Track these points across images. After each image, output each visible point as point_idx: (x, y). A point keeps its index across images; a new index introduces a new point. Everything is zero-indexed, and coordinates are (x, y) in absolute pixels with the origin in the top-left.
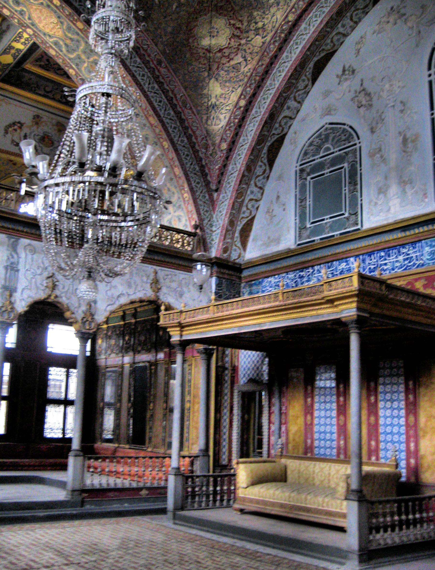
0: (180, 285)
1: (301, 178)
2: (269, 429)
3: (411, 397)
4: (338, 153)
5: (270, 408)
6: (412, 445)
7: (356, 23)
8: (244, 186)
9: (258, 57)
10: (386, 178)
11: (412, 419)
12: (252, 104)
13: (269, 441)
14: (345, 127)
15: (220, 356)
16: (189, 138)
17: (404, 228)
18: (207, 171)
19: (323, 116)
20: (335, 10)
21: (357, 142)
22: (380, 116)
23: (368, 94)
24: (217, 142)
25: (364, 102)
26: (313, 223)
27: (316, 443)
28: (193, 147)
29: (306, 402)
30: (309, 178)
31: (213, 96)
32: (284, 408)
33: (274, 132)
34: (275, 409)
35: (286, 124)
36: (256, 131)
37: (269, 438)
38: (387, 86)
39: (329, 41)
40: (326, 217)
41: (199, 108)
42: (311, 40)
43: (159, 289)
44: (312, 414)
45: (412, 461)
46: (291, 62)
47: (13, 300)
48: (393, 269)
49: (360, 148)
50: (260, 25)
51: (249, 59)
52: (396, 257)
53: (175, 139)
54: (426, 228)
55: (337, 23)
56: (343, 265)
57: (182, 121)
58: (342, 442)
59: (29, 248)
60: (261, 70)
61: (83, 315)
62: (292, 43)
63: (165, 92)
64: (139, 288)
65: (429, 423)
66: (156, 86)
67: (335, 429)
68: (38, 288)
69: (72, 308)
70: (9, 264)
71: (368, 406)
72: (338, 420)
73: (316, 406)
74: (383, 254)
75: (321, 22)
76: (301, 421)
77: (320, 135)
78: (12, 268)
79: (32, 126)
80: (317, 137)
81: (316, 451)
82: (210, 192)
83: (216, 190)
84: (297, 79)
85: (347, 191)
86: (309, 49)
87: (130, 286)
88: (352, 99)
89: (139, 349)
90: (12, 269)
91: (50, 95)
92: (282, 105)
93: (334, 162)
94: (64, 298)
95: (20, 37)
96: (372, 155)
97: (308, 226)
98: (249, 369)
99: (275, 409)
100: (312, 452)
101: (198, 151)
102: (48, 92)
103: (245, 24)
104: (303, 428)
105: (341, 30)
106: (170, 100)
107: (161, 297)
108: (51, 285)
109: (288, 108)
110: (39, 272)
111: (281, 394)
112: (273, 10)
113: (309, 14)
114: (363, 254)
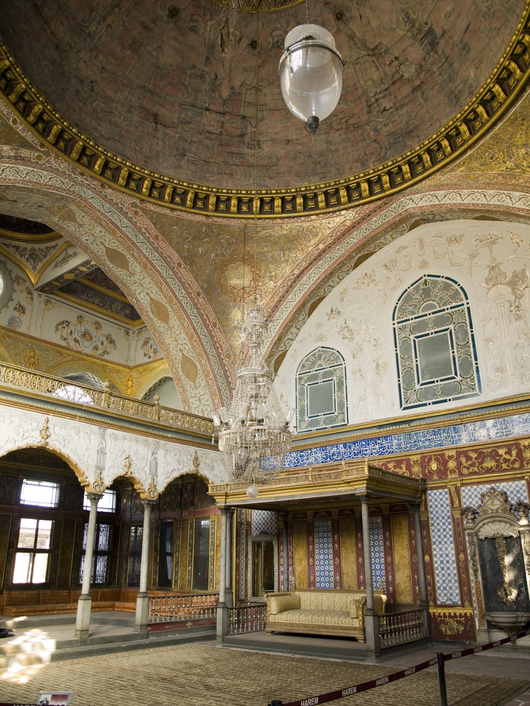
0: (212, 461)
2: (279, 569)
3: (388, 543)
4: (329, 369)
5: (279, 553)
6: (390, 577)
7: (341, 280)
9: (270, 296)
10: (365, 391)
11: (389, 559)
13: (279, 579)
15: (239, 514)
16: (217, 349)
17: (380, 427)
18: (228, 374)
19: (316, 341)
20: (329, 272)
21: (343, 363)
22: (360, 347)
23: (350, 330)
24: (237, 353)
25: (347, 336)
26: (310, 417)
27: (317, 579)
28: (219, 356)
29: (308, 548)
31: (236, 320)
32: (290, 553)
33: (280, 349)
34: (284, 554)
35: (288, 343)
37: (279, 577)
38: (364, 327)
39: (322, 290)
41: (225, 328)
42: (311, 290)
43: (198, 465)
44: (313, 558)
45: (391, 588)
47: (102, 476)
48: (372, 454)
50: (273, 274)
52: (374, 446)
53: (208, 351)
54: (394, 428)
55: (329, 280)
56: (335, 449)
57: (212, 337)
58: (338, 578)
59: (112, 436)
60: (272, 304)
61: (149, 487)
62: (296, 288)
63: (201, 315)
64: (186, 465)
65: (401, 561)
66: (196, 311)
67: (332, 568)
68: (119, 467)
69: (142, 482)
70: (99, 448)
71: (357, 551)
72: (334, 561)
73: (317, 551)
74: (364, 443)
75: (318, 278)
76: (305, 563)
77: (315, 354)
78: (102, 452)
79: (76, 325)
80: (312, 356)
81: (318, 585)
84: (299, 314)
86: (309, 295)
87: (179, 463)
88: (339, 332)
89: (165, 508)
90: (102, 452)
91: (91, 300)
92: (287, 331)
93: (325, 375)
94: (136, 474)
95: (87, 264)
96: (354, 373)
97: (306, 419)
98: (260, 524)
99: (284, 554)
100: (314, 586)
101: (223, 359)
102: (89, 298)
103: (263, 272)
104: (306, 568)
105: (331, 284)
106: (204, 321)
107: (200, 471)
108: (128, 464)
109: (291, 333)
110: (119, 454)
111: (288, 543)
112: (283, 265)
114: (349, 443)
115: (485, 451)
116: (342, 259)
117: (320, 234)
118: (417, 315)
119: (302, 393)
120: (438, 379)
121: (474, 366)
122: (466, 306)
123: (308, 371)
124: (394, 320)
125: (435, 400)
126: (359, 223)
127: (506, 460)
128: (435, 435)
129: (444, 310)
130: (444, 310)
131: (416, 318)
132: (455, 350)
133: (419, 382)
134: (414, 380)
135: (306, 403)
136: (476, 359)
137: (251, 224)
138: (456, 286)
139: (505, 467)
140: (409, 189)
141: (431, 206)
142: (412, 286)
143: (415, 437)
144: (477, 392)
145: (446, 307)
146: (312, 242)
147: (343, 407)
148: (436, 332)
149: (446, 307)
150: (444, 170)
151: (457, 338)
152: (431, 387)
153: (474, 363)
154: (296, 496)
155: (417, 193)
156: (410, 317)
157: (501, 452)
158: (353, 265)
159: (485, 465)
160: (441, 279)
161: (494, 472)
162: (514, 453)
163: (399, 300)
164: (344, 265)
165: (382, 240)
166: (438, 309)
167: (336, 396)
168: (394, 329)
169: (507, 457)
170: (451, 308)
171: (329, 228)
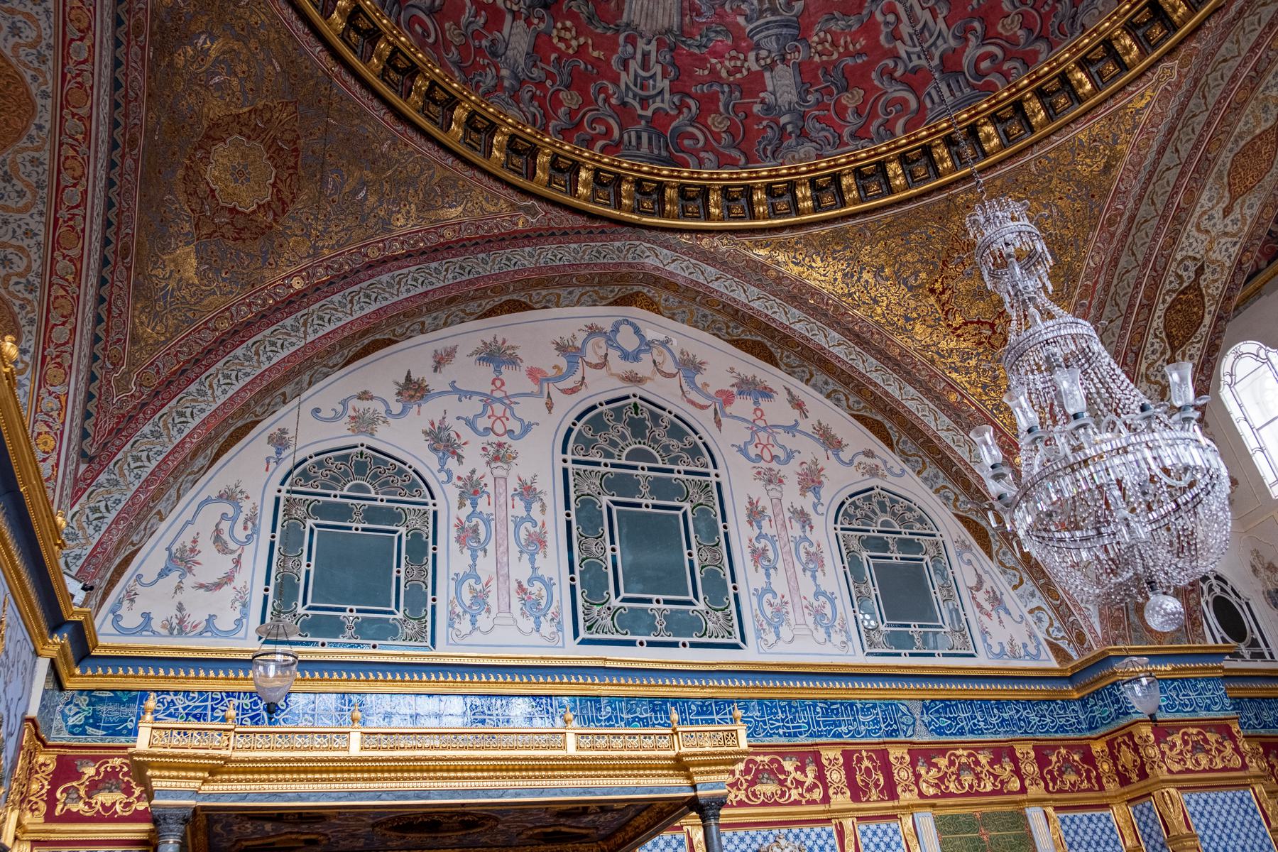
1: (287, 512)
7: (446, 325)
8: (171, 480)
12: (237, 338)
14: (406, 468)
20: (454, 293)
21: (431, 502)
30: (310, 522)
36: (243, 389)
40: (349, 607)
46: (350, 319)
49: (435, 513)
51: (272, 261)
77: (345, 458)
80: (337, 459)
82: (83, 455)
83: (91, 460)
85: (402, 575)
92: (299, 373)
93: (372, 514)
97: (301, 610)
105: (428, 321)
113: (400, 268)
115: (758, 759)
116: (490, 283)
117: (460, 209)
118: (616, 461)
119: (292, 539)
120: (661, 597)
121: (731, 591)
122: (713, 479)
123: (319, 490)
124: (564, 451)
125: (652, 638)
126: (541, 235)
127: (800, 784)
128: (653, 710)
129: (671, 471)
130: (671, 471)
131: (613, 466)
132: (694, 551)
133: (617, 594)
134: (607, 587)
135: (304, 568)
136: (734, 580)
137: (344, 83)
138: (696, 438)
139: (798, 798)
140: (654, 233)
141: (692, 281)
142: (608, 403)
143: (609, 709)
144: (738, 641)
145: (676, 468)
146: (432, 215)
147: (419, 601)
148: (655, 506)
149: (676, 468)
150: (729, 236)
151: (696, 531)
152: (645, 610)
153: (730, 585)
154: (504, 792)
155: (666, 248)
156: (603, 460)
157: (789, 765)
158: (489, 307)
159: (758, 788)
160: (666, 413)
161: (776, 804)
162: (811, 771)
163: (579, 418)
164: (481, 298)
165: (563, 293)
166: (660, 465)
167: (401, 572)
168: (565, 471)
169: (799, 776)
170: (686, 472)
171: (482, 209)
